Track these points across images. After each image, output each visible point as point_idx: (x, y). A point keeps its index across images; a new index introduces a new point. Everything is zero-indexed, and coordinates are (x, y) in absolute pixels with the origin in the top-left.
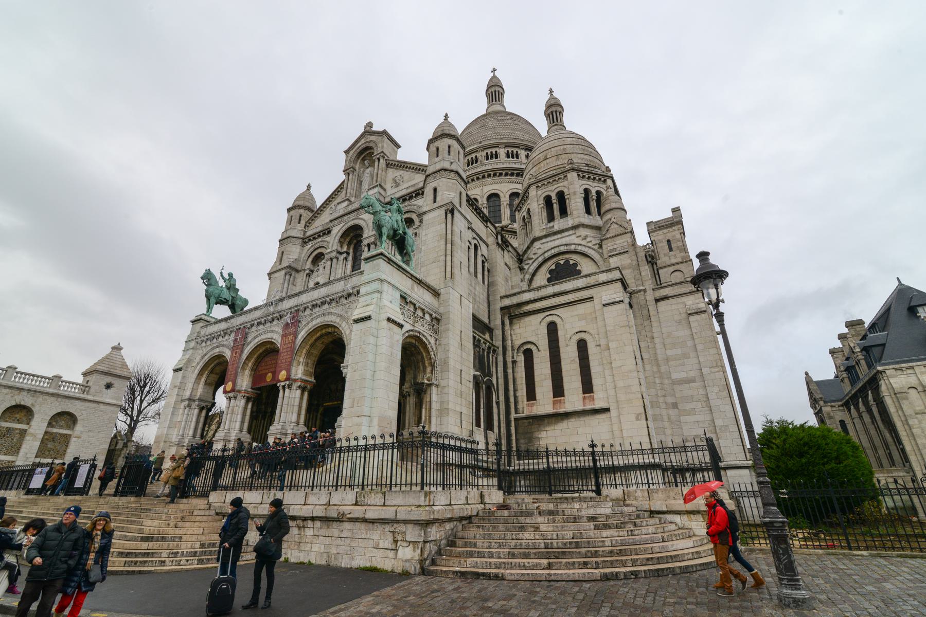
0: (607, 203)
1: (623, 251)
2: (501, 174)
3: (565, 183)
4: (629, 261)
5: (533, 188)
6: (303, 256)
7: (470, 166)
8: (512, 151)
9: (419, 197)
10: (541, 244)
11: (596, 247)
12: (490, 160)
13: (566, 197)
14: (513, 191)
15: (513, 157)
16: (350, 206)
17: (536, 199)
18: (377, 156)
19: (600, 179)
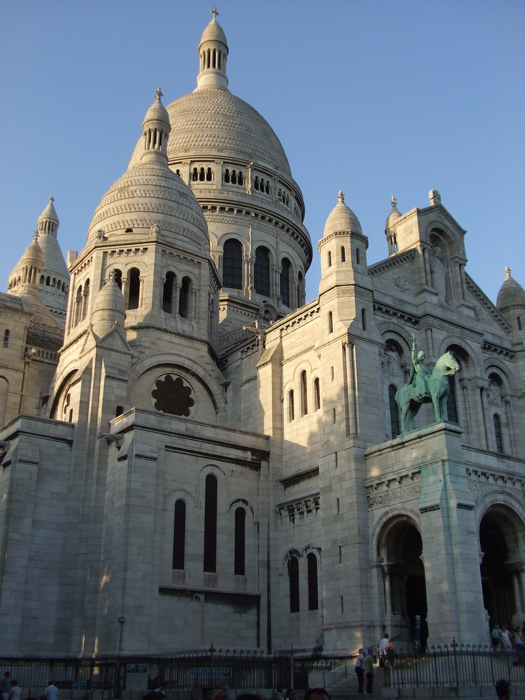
9: (507, 358)
16: (449, 312)
18: (462, 262)
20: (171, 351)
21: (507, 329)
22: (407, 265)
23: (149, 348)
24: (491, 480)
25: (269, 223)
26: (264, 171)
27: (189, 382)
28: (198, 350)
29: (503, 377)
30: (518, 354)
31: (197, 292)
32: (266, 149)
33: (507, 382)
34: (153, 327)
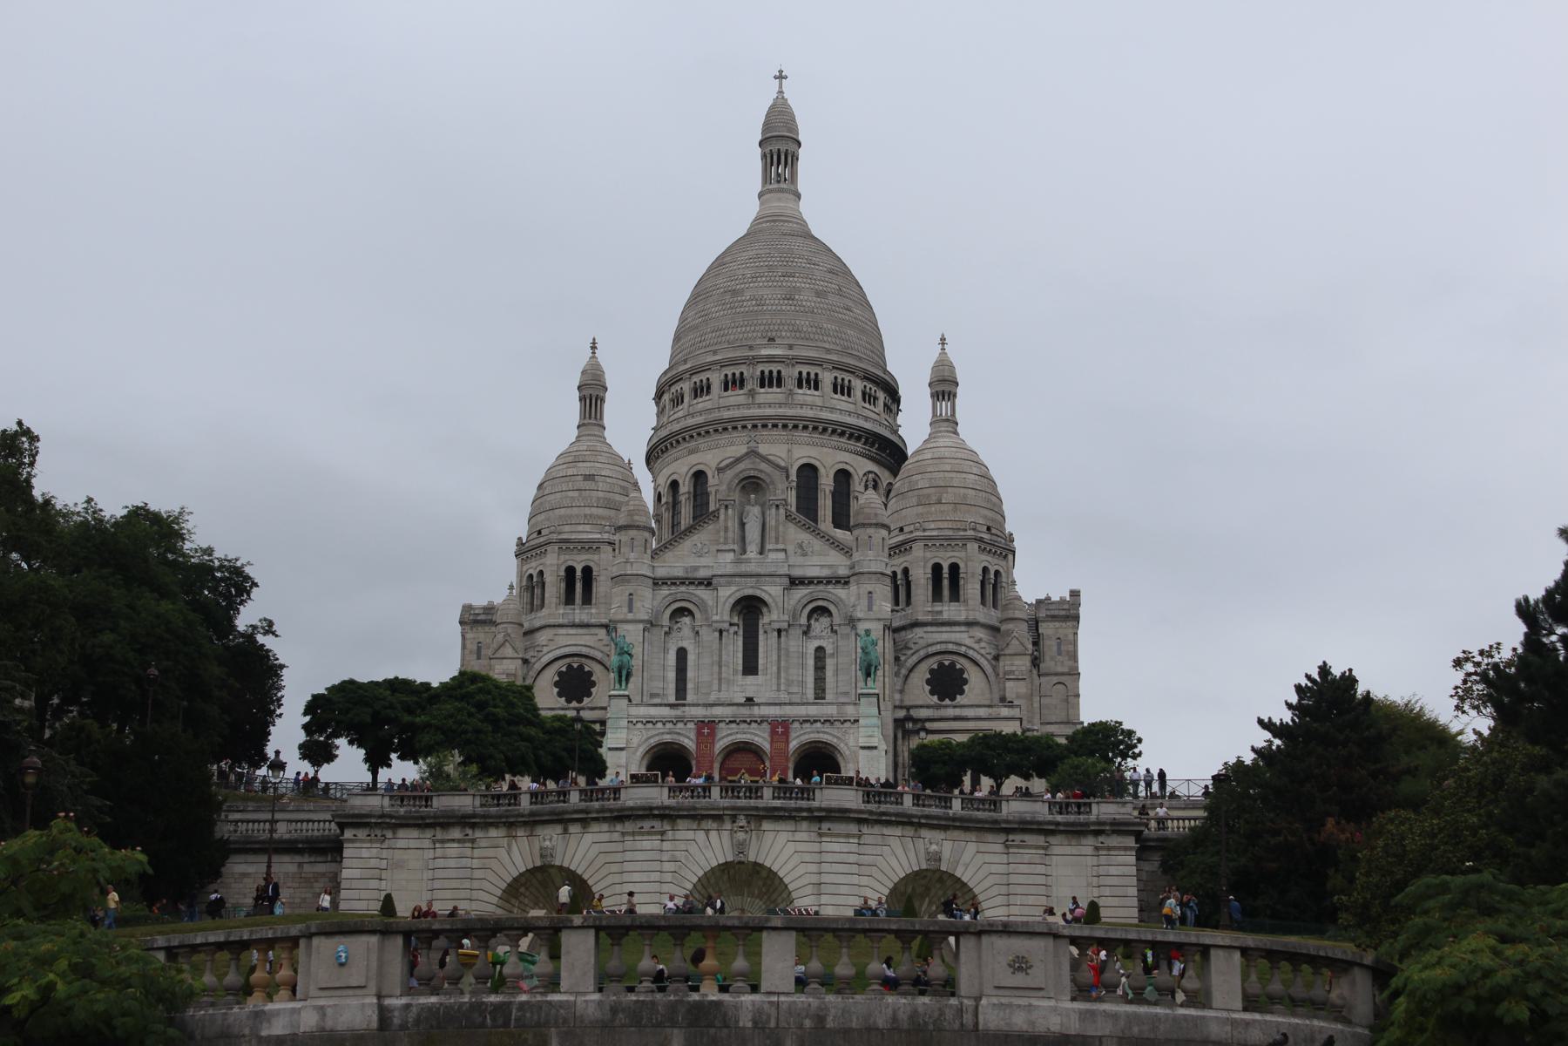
0: (1011, 609)
1: (1020, 677)
2: (825, 430)
3: (963, 554)
4: (1025, 690)
5: (921, 544)
6: (655, 603)
7: (766, 389)
8: (843, 379)
9: (839, 586)
10: (925, 632)
11: (989, 657)
12: (805, 390)
13: (961, 575)
14: (841, 466)
15: (843, 395)
16: (743, 565)
17: (922, 564)
18: (778, 503)
19: (1001, 553)
20: (568, 643)
21: (846, 551)
22: (710, 527)
23: (546, 646)
24: (660, 725)
25: (775, 429)
26: (771, 359)
27: (589, 666)
28: (596, 635)
29: (832, 608)
30: (852, 579)
31: (598, 578)
32: (783, 322)
33: (836, 610)
34: (550, 626)
